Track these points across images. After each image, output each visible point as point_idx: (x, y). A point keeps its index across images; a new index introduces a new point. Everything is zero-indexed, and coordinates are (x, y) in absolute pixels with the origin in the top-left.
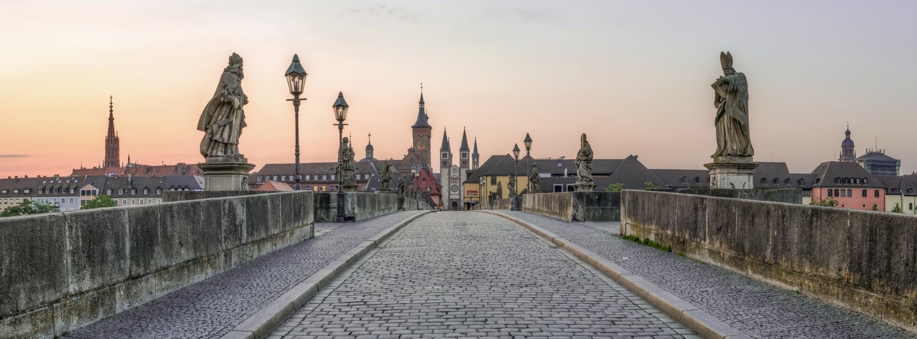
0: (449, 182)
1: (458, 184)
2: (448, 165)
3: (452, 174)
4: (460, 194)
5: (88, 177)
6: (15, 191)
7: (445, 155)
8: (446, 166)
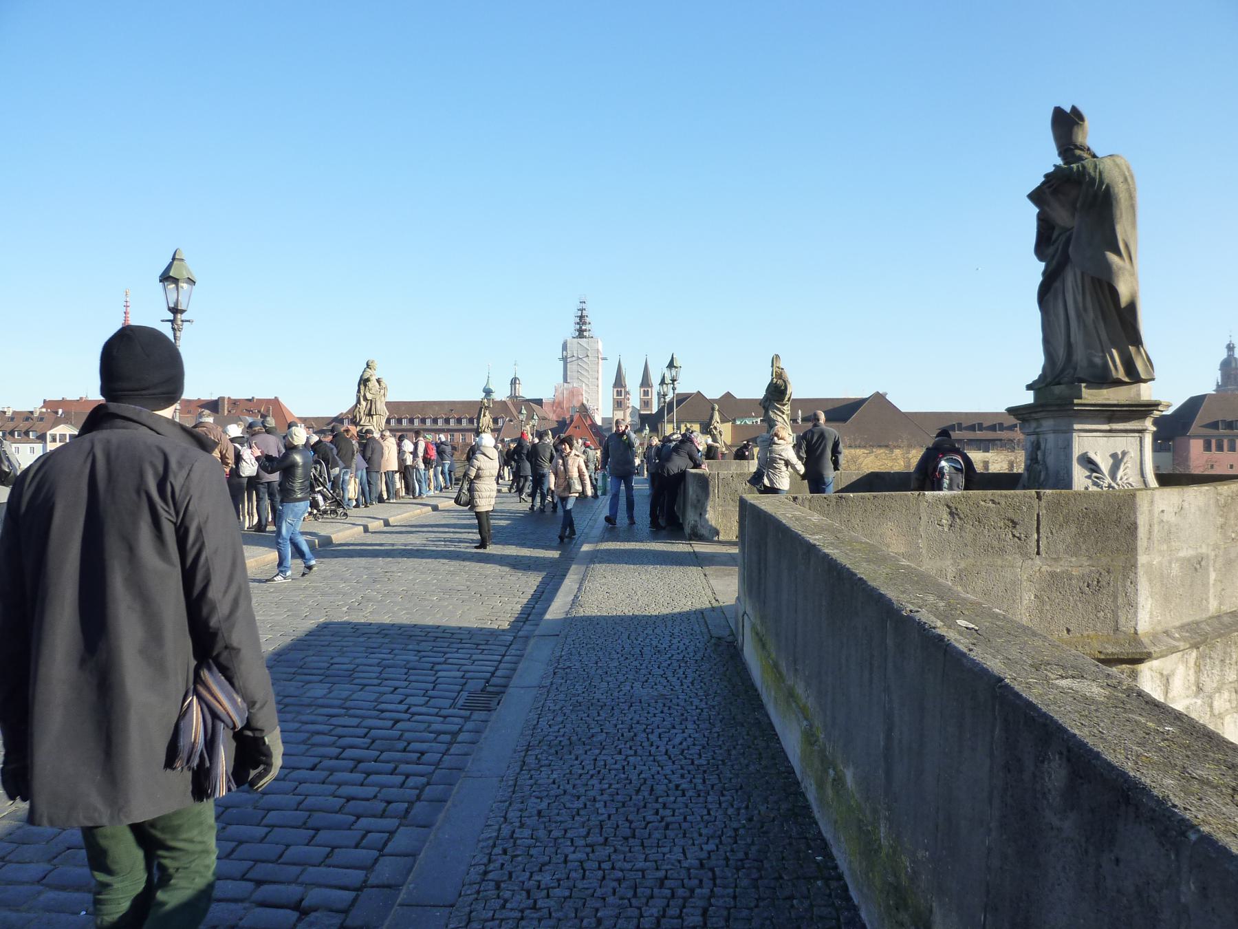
2: (623, 407)
5: (63, 412)
7: (619, 393)
8: (621, 407)
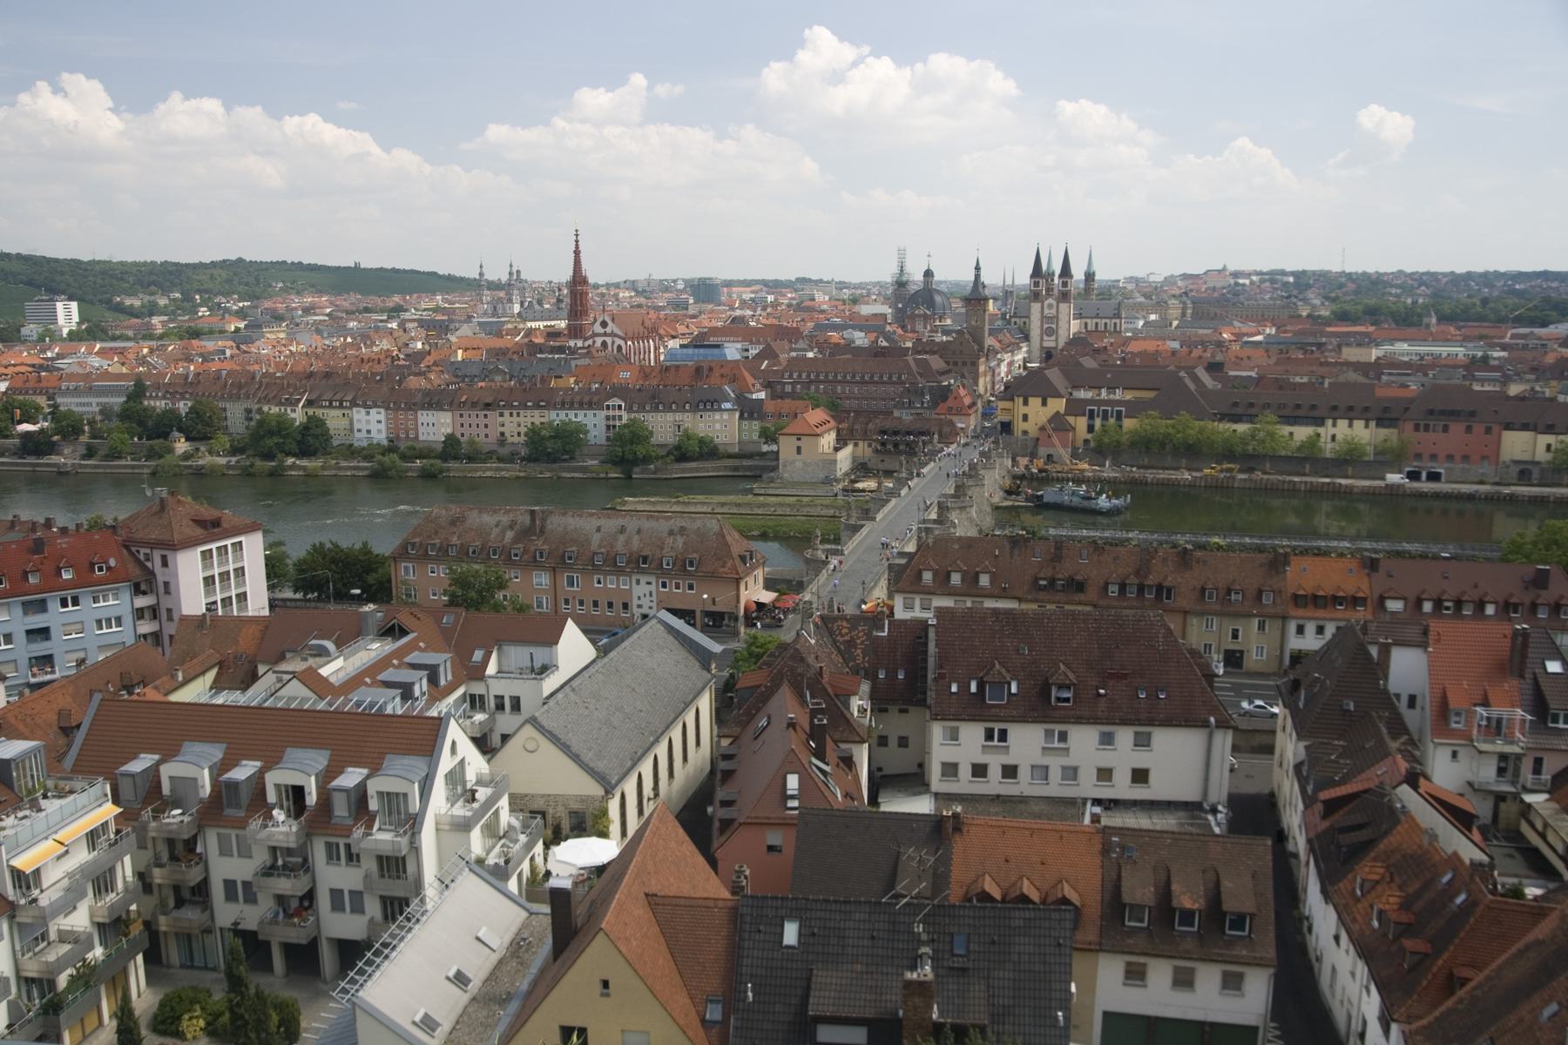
0: (1042, 322)
1: (1054, 326)
3: (1046, 311)
4: (1057, 340)
6: (515, 404)
